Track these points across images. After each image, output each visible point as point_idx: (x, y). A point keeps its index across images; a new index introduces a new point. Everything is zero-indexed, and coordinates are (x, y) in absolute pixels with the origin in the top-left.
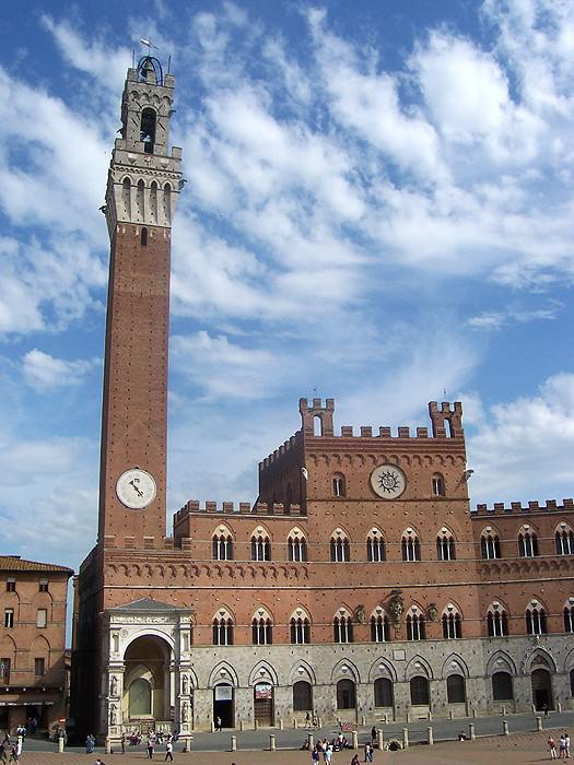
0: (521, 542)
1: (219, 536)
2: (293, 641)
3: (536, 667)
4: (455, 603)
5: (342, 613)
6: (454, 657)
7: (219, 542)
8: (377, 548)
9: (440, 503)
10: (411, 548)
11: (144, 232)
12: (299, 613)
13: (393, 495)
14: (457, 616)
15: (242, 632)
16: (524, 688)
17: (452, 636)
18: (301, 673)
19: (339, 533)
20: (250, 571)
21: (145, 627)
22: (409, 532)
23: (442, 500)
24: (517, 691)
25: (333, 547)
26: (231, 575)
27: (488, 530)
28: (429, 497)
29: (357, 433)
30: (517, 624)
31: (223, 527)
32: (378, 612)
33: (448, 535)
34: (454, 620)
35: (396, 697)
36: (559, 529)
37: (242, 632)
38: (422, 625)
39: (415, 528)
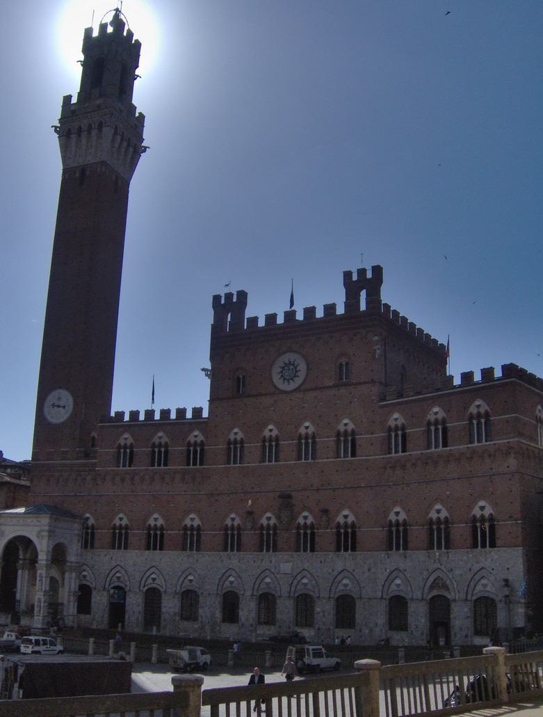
0: (429, 431)
1: (122, 444)
2: (184, 549)
3: (435, 593)
4: (350, 508)
5: (233, 519)
6: (345, 573)
7: (122, 450)
8: (271, 448)
9: (343, 390)
10: (307, 446)
11: (83, 171)
12: (192, 519)
13: (293, 386)
14: (353, 525)
15: (137, 535)
16: (419, 617)
17: (346, 550)
18: (191, 581)
19: (236, 434)
20: (147, 477)
21: (17, 528)
22: (307, 427)
23: (345, 385)
24: (411, 619)
25: (229, 449)
26: (132, 479)
27: (396, 418)
28: (331, 384)
29: (262, 323)
30: (418, 534)
31: (126, 435)
32: (268, 519)
33: (351, 426)
34: (350, 530)
35: (278, 616)
36: (473, 410)
37: (137, 535)
38: (313, 534)
39: (313, 422)
